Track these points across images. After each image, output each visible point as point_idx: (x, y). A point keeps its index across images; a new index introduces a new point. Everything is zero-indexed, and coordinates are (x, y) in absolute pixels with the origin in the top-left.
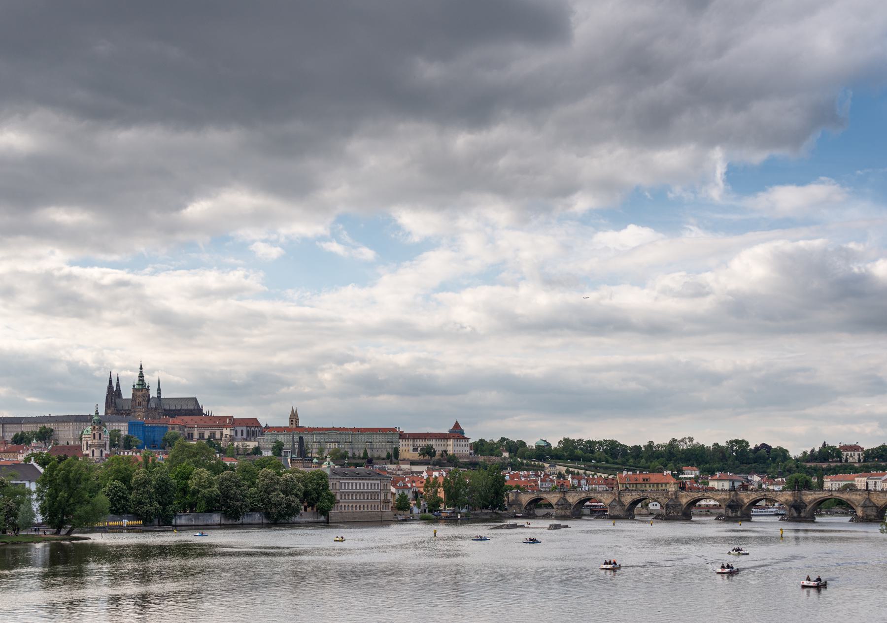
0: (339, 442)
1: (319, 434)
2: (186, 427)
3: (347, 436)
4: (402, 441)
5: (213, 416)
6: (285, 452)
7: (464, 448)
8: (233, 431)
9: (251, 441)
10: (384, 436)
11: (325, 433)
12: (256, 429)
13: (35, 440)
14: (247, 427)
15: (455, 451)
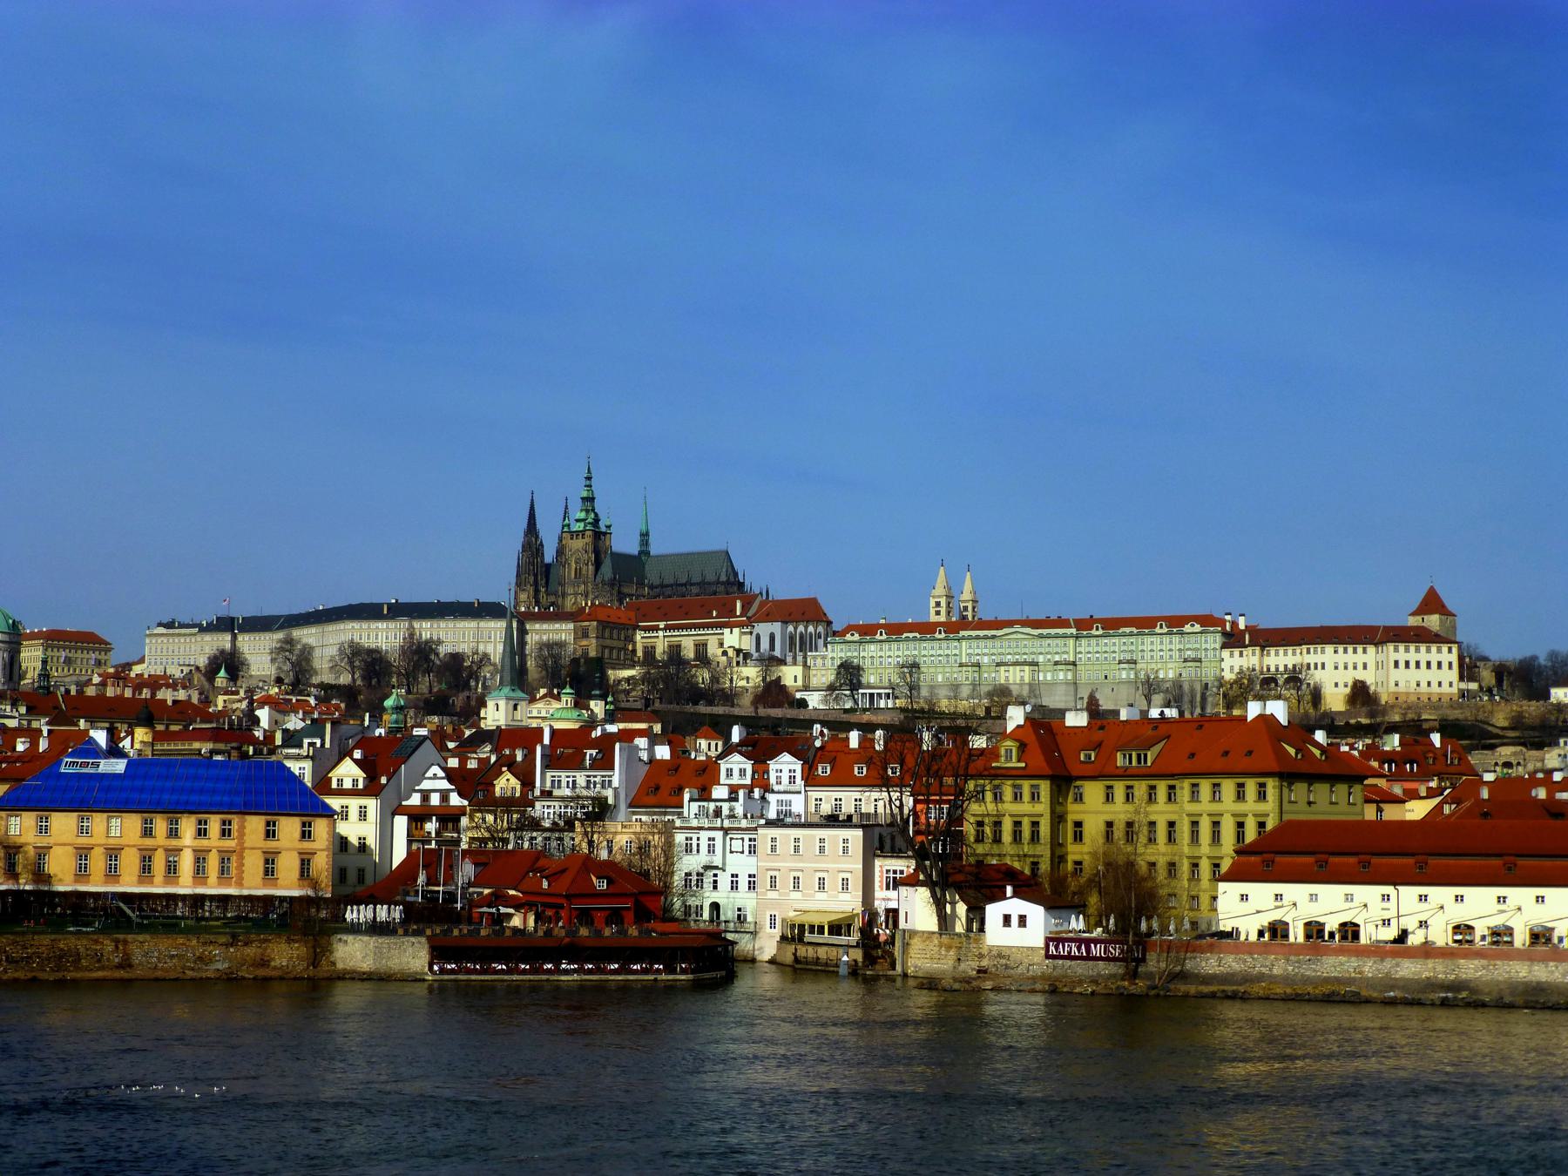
0: (1036, 664)
1: (978, 637)
2: (637, 627)
3: (1059, 641)
4: (1232, 655)
5: (770, 599)
6: (862, 694)
7: (1434, 675)
8: (747, 638)
9: (795, 663)
10: (1176, 639)
11: (994, 637)
12: (811, 629)
13: (223, 671)
14: (785, 622)
15: (1397, 685)
